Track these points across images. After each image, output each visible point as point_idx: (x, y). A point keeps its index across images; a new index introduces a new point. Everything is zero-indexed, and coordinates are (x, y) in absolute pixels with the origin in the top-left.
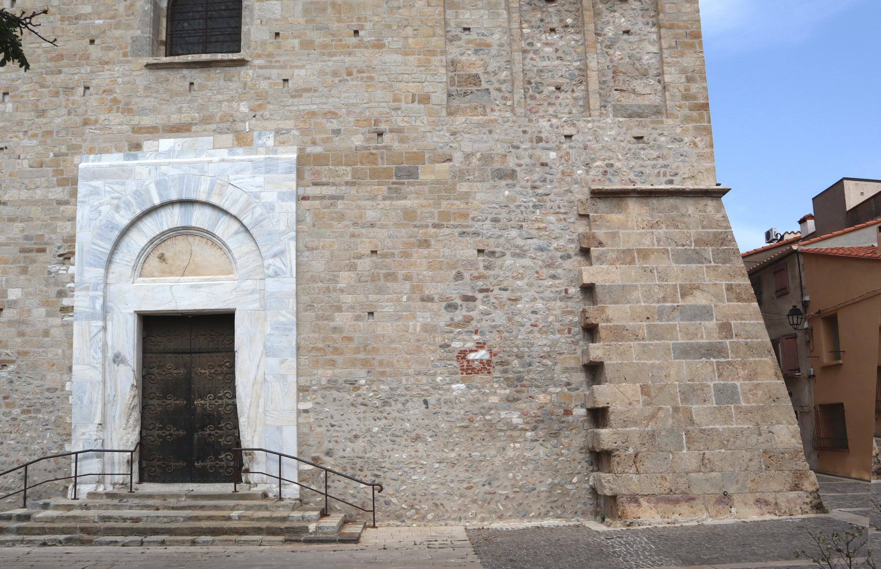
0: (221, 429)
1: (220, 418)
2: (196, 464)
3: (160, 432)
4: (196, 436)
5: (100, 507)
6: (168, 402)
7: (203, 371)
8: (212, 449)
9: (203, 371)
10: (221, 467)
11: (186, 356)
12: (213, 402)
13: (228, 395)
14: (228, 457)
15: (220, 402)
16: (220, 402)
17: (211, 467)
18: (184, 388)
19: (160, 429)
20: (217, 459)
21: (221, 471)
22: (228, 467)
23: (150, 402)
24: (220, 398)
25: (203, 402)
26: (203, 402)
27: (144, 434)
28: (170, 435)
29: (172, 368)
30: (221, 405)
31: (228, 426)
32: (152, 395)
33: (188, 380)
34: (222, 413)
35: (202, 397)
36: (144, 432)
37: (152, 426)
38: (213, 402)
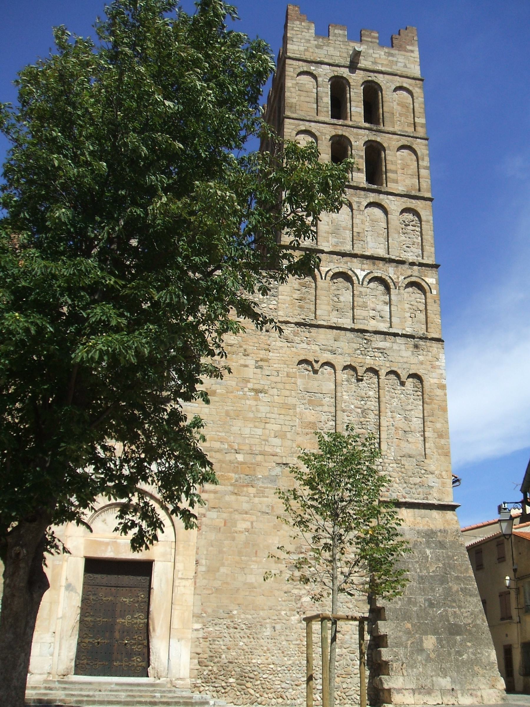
3: (91, 640)
7: (125, 600)
9: (125, 600)
18: (111, 610)
23: (86, 619)
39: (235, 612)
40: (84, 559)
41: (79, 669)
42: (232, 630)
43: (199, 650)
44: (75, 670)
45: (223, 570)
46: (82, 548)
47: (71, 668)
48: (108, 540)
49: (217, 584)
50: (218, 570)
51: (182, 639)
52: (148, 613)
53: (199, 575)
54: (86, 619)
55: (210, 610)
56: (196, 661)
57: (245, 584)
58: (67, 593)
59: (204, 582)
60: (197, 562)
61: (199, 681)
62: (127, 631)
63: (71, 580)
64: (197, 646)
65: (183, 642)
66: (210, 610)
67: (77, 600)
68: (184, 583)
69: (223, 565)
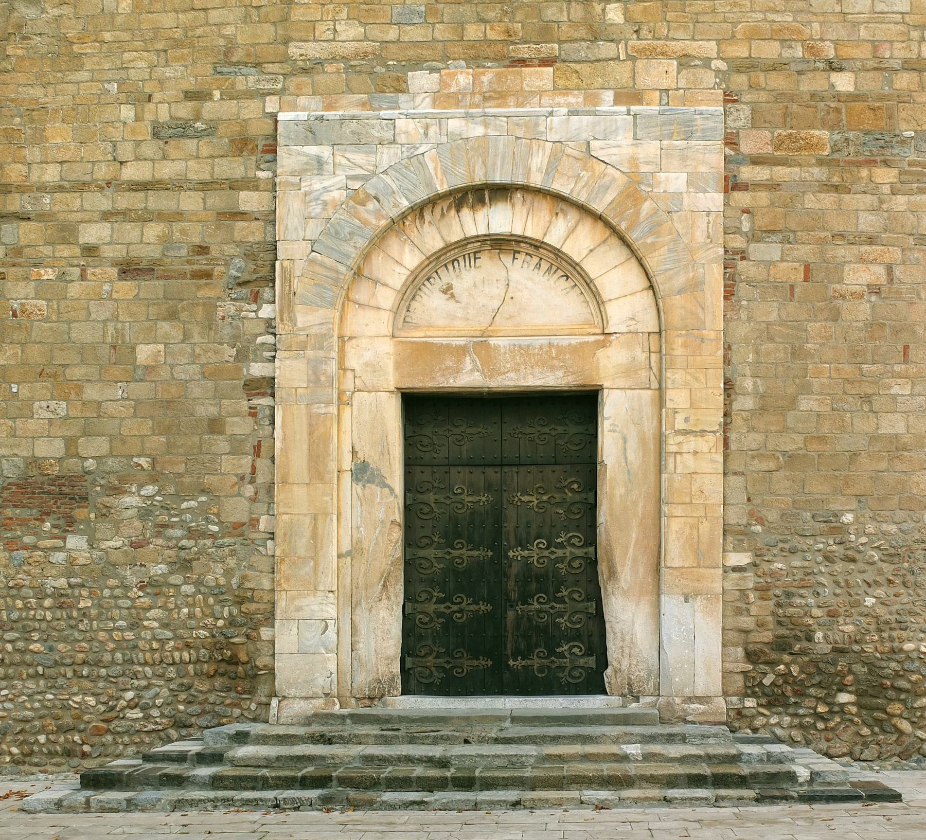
0: (561, 601)
1: (559, 583)
2: (511, 663)
3: (441, 608)
4: (511, 614)
6: (456, 553)
7: (526, 498)
8: (550, 638)
9: (526, 498)
10: (561, 668)
11: (490, 471)
12: (546, 553)
14: (576, 650)
15: (560, 553)
16: (560, 553)
18: (489, 529)
20: (552, 652)
21: (561, 675)
23: (422, 553)
24: (561, 546)
29: (467, 494)
30: (561, 560)
31: (576, 596)
33: (497, 515)
34: (563, 572)
35: (523, 544)
38: (546, 553)
39: (848, 518)
40: (400, 395)
41: (412, 682)
42: (839, 567)
43: (747, 622)
44: (405, 682)
45: (806, 404)
46: (390, 365)
47: (392, 679)
48: (461, 342)
49: (792, 443)
50: (793, 403)
52: (591, 538)
53: (737, 421)
54: (422, 553)
55: (772, 516)
56: (740, 651)
57: (874, 438)
59: (753, 440)
60: (729, 387)
61: (750, 703)
62: (542, 581)
64: (739, 612)
66: (772, 516)
67: (389, 502)
68: (692, 443)
69: (806, 389)
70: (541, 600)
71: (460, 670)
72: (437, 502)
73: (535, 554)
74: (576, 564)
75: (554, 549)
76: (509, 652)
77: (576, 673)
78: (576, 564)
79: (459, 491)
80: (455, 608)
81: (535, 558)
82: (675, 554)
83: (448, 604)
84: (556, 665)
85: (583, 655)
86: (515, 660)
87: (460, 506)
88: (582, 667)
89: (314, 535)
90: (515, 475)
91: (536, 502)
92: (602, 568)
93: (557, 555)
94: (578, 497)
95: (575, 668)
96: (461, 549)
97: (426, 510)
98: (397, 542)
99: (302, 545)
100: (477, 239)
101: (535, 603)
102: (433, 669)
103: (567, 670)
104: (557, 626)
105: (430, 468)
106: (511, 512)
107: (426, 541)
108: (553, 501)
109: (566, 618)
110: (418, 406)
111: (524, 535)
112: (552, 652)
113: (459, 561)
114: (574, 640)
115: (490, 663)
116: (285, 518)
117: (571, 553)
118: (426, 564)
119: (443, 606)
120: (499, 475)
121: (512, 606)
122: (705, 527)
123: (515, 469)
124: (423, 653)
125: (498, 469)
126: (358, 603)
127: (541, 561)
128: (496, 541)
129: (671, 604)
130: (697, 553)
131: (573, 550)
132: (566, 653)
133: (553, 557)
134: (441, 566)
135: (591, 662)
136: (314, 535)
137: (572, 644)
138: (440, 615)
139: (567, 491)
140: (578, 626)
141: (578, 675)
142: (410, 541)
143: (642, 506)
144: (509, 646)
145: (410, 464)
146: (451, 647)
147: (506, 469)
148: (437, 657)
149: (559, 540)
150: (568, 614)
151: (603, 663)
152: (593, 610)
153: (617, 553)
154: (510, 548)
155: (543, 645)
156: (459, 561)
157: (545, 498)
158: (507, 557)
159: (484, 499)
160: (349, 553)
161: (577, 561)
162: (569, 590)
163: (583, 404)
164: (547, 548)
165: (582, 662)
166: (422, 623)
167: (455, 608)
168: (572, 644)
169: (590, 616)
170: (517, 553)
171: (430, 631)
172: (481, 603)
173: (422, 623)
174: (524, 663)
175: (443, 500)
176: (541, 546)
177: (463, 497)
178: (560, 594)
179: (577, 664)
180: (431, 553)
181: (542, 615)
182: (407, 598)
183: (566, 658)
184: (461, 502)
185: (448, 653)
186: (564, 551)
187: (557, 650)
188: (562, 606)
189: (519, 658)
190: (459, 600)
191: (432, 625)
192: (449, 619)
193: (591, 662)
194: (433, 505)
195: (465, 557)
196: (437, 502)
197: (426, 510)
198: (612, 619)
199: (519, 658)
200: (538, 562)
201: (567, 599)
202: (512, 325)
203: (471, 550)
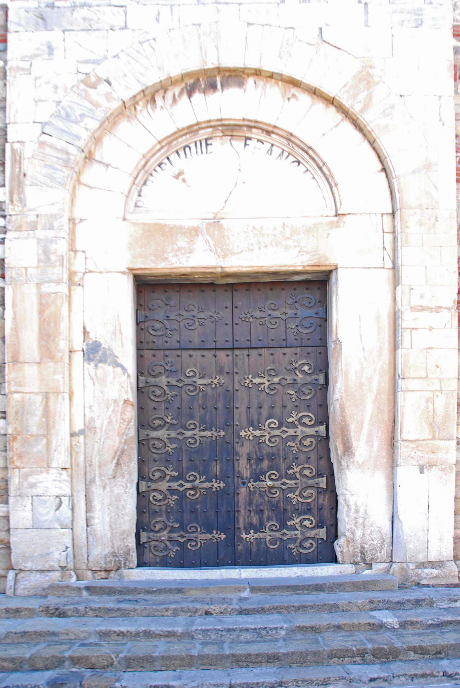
0: (293, 477)
2: (244, 536)
3: (175, 485)
4: (243, 491)
5: (99, 613)
7: (257, 380)
9: (257, 380)
10: (293, 540)
11: (221, 355)
12: (277, 432)
13: (306, 420)
14: (307, 523)
15: (291, 432)
16: (291, 432)
17: (274, 541)
19: (174, 479)
20: (283, 525)
21: (292, 546)
22: (307, 539)
23: (154, 434)
25: (258, 433)
26: (258, 433)
27: (143, 488)
28: (193, 488)
31: (307, 472)
32: (158, 422)
33: (229, 396)
35: (253, 424)
36: (143, 485)
37: (158, 475)
38: (277, 432)
51: (431, 465)
54: (154, 434)
58: (90, 367)
63: (98, 334)
65: (434, 473)
70: (273, 477)
71: (194, 544)
72: (169, 385)
73: (268, 433)
74: (307, 442)
75: (284, 428)
76: (241, 525)
77: (307, 544)
78: (307, 442)
79: (191, 374)
80: (188, 485)
81: (267, 438)
82: (411, 426)
83: (181, 482)
84: (287, 537)
85: (314, 527)
86: (248, 533)
87: (192, 388)
88: (312, 538)
89: (46, 413)
90: (246, 359)
91: (267, 383)
92: (336, 444)
93: (288, 434)
94: (309, 379)
95: (307, 539)
96: (193, 429)
97: (158, 392)
98: (129, 422)
99: (34, 423)
100: (209, 124)
101: (267, 480)
102: (168, 543)
103: (298, 541)
104: (289, 500)
105: (162, 352)
106: (242, 394)
107: (158, 422)
108: (284, 383)
109: (297, 493)
110: (147, 287)
111: (255, 417)
112: (283, 525)
113: (192, 441)
114: (305, 513)
115: (223, 536)
116: (17, 396)
117: (302, 432)
118: (159, 444)
119: (176, 484)
120: (230, 358)
121: (244, 483)
122: (440, 402)
123: (246, 352)
124: (157, 528)
125: (229, 352)
126: (93, 481)
127: (273, 440)
128: (228, 423)
129: (406, 474)
130: (432, 426)
131: (304, 429)
132: (297, 526)
133: (284, 436)
134: (174, 446)
135: (322, 533)
136: (46, 413)
137: (303, 517)
138: (172, 491)
139: (297, 373)
140: (309, 501)
141: (309, 545)
142: (142, 424)
143: (378, 382)
144: (241, 520)
145: (141, 347)
146: (185, 522)
147: (237, 352)
148: (171, 532)
149: (291, 420)
150: (299, 489)
151: (334, 534)
152: (323, 485)
153: (353, 428)
154: (241, 428)
155: (274, 519)
156: (192, 441)
157: (276, 380)
158: (239, 437)
159: (216, 381)
160: (82, 432)
161: (309, 440)
162: (300, 467)
163: (318, 284)
164: (279, 428)
165: (313, 533)
166: (156, 500)
167: (188, 485)
168: (303, 517)
169: (320, 491)
170: (249, 433)
171: (164, 508)
172: (214, 480)
173: (156, 500)
174: (256, 536)
175: (174, 383)
176: (272, 425)
177: (194, 379)
178: (291, 471)
179: (308, 535)
180: (161, 434)
181: (273, 491)
182: (141, 476)
183: (297, 530)
184: (193, 384)
185: (183, 528)
186: (296, 430)
187: (289, 523)
188: (293, 482)
189: (252, 531)
190: (192, 478)
191: (166, 502)
192: (182, 495)
193: (322, 533)
194: (165, 388)
195: (197, 437)
196: (169, 385)
197: (158, 392)
198: (345, 492)
199: (252, 531)
200: (269, 440)
201: (298, 476)
202: (244, 219)
203: (204, 430)
